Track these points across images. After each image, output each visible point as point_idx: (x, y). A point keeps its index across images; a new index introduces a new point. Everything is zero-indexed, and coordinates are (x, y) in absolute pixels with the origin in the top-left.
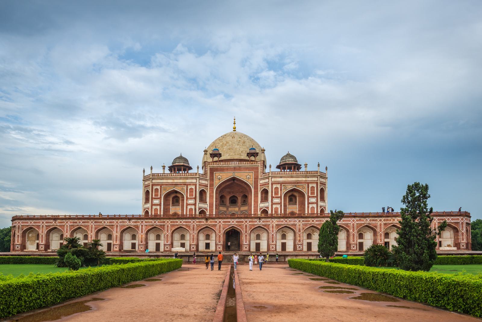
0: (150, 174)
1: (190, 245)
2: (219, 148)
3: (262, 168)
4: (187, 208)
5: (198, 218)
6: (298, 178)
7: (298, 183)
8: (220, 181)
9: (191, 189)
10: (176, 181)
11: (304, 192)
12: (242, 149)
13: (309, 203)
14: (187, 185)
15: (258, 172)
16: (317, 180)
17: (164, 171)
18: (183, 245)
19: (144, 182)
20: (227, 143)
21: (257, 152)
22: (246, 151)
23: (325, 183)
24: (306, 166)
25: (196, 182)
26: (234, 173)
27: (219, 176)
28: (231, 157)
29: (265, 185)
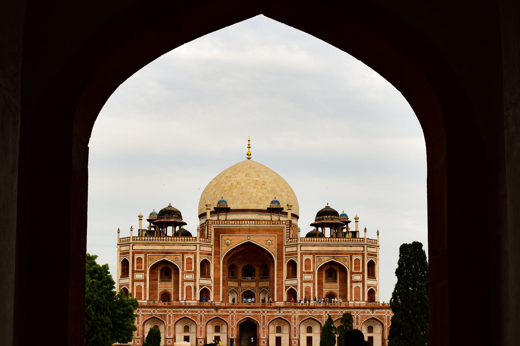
1: (197, 339)
2: (225, 191)
4: (183, 285)
7: (337, 254)
8: (229, 247)
10: (167, 248)
12: (261, 194)
13: (352, 282)
14: (183, 254)
17: (140, 225)
18: (187, 339)
19: (119, 246)
22: (267, 198)
29: (293, 254)
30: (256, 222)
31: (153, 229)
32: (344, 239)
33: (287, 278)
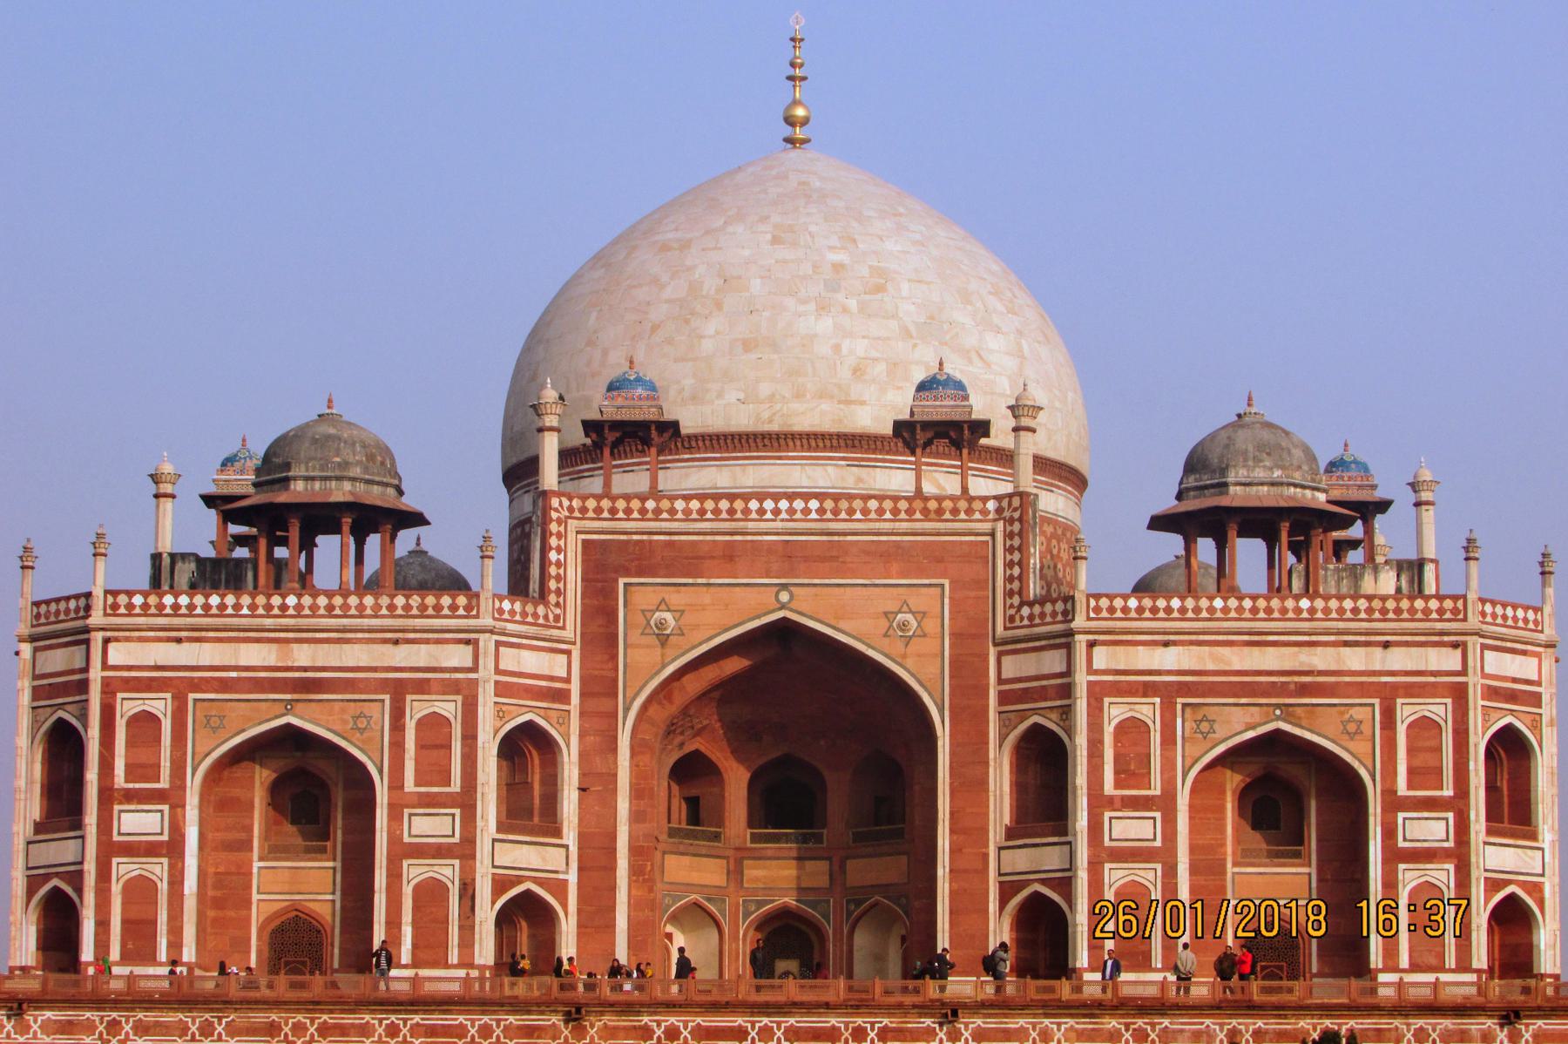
0: (88, 595)
3: (1016, 557)
4: (395, 876)
5: (517, 1006)
6: (1306, 649)
7: (1304, 690)
8: (670, 653)
9: (433, 725)
11: (1356, 764)
12: (860, 347)
13: (1394, 856)
14: (399, 689)
15: (980, 584)
16: (1459, 667)
19: (26, 649)
20: (728, 282)
21: (976, 416)
22: (896, 367)
23: (1539, 684)
24: (1425, 496)
25: (469, 663)
26: (784, 587)
28: (766, 415)
29: (1042, 694)
30: (829, 504)
31: (242, 552)
32: (1348, 604)
33: (1011, 833)
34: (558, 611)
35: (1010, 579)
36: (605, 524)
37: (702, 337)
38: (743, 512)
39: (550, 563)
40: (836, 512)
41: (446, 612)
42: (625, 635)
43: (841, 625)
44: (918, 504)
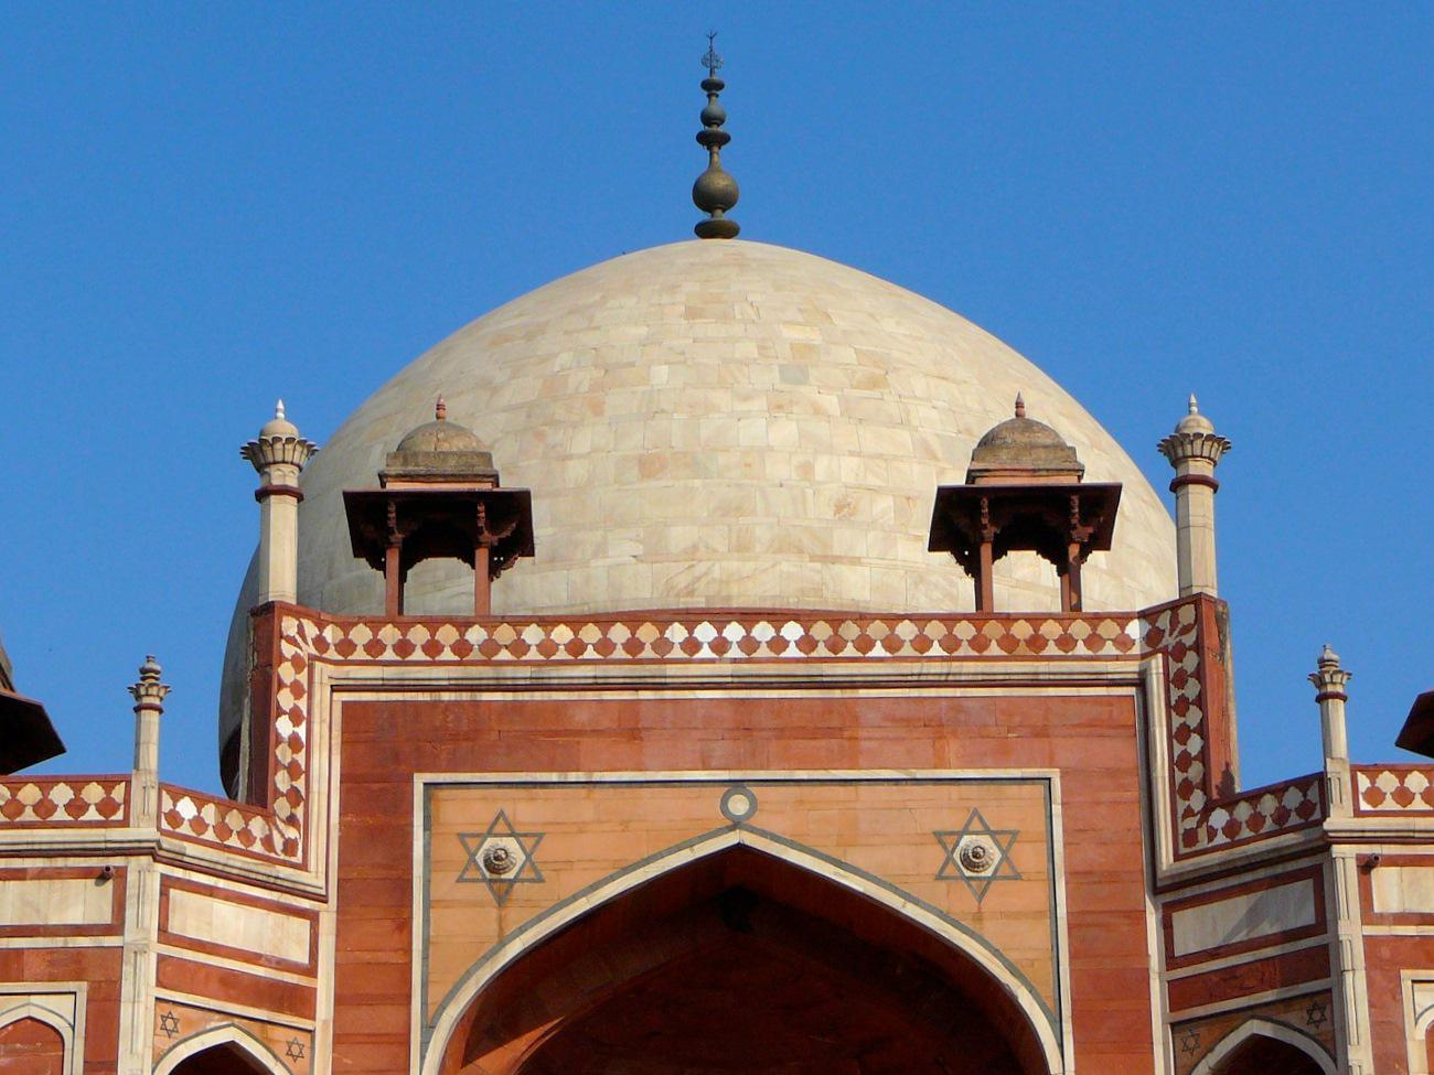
8: (515, 916)
12: (848, 469)
25: (106, 918)
27: (490, 833)
28: (682, 581)
30: (821, 631)
34: (292, 833)
35: (1181, 762)
36: (390, 672)
37: (570, 457)
38: (655, 646)
39: (279, 740)
40: (835, 645)
41: (61, 815)
42: (427, 883)
43: (852, 857)
44: (993, 629)
